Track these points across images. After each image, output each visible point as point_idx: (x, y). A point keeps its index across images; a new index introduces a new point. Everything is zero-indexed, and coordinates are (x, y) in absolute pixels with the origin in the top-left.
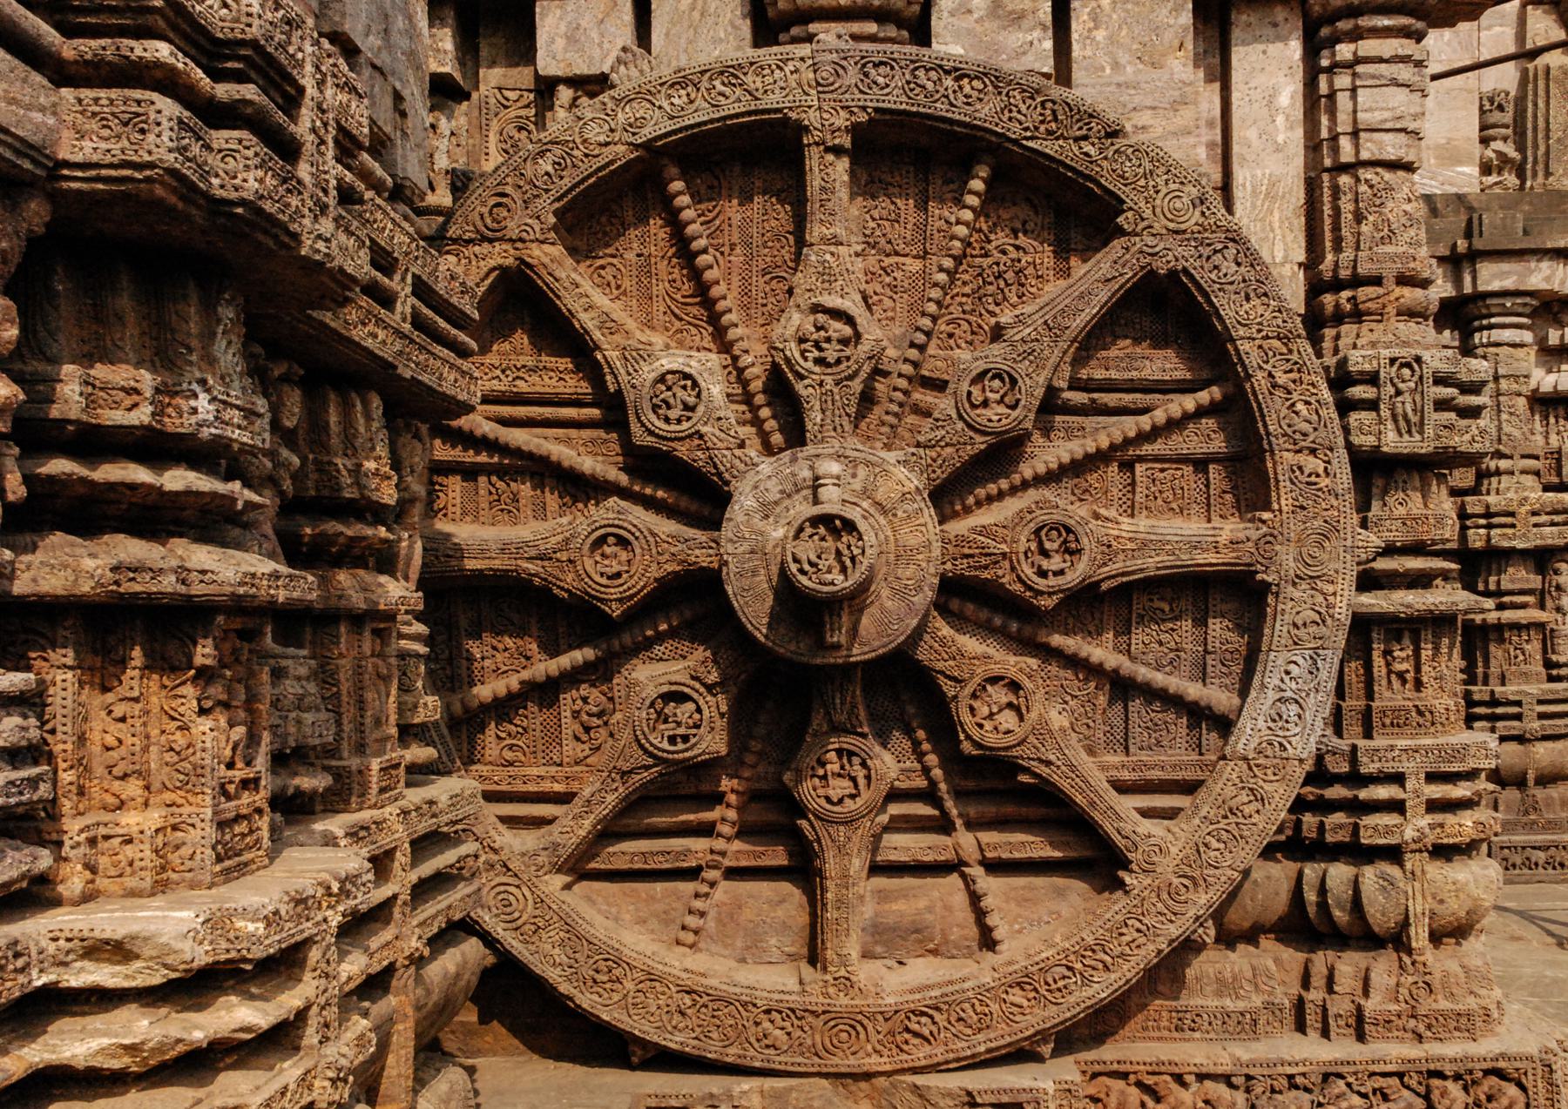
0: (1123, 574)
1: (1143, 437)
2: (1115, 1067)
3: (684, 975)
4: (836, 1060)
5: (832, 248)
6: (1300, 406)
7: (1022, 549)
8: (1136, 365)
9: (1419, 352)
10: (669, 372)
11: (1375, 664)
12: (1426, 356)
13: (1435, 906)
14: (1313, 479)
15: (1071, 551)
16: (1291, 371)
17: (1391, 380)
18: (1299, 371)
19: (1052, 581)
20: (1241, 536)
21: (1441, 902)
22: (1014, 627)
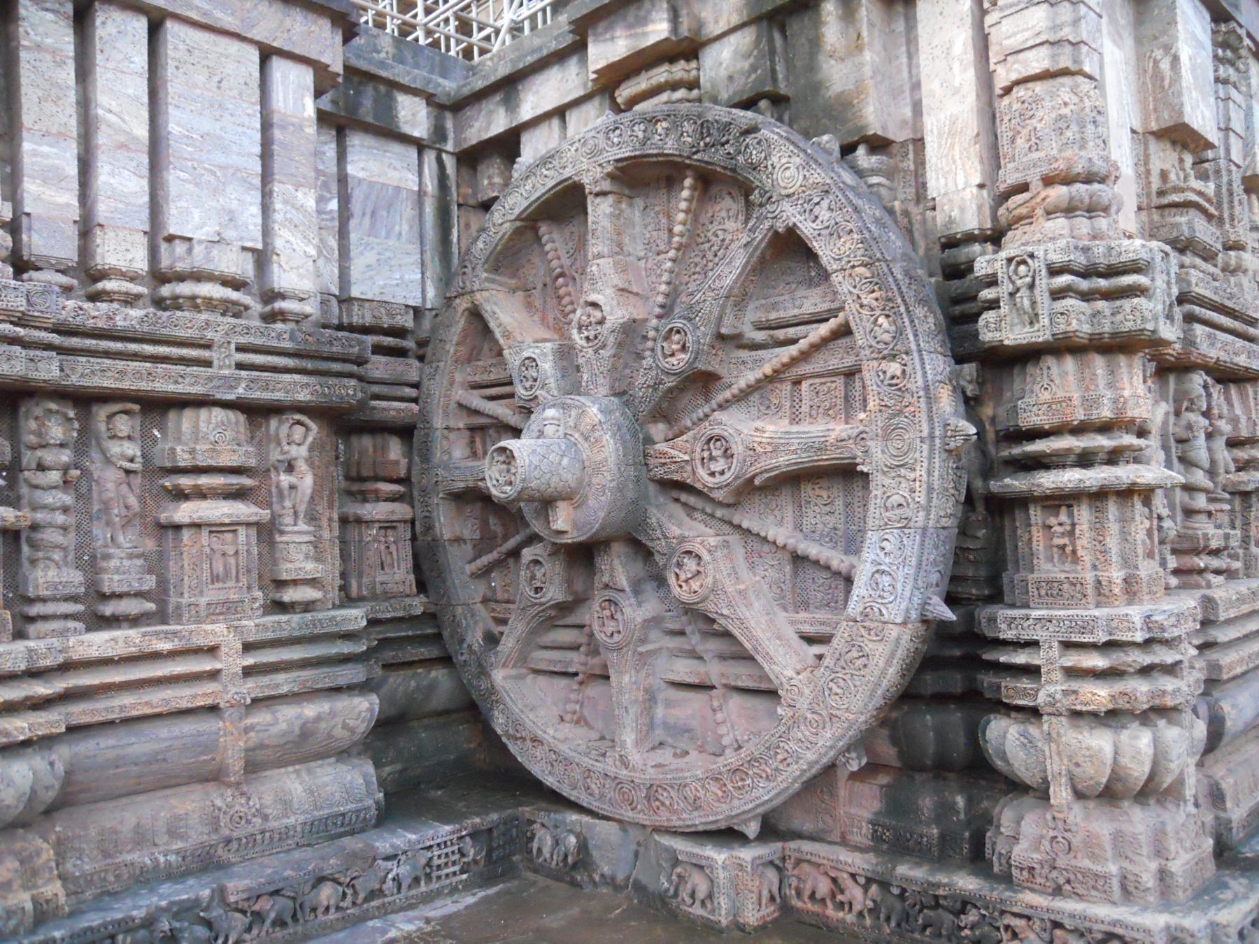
0: (766, 471)
1: (794, 361)
2: (809, 857)
3: (551, 740)
4: (623, 812)
5: (598, 261)
6: (881, 320)
7: (697, 456)
8: (797, 303)
9: (1030, 249)
10: (528, 358)
11: (1035, 539)
12: (1039, 252)
13: (1072, 768)
14: (894, 381)
15: (727, 454)
16: (873, 291)
17: (1010, 278)
18: (880, 289)
19: (718, 479)
20: (844, 435)
21: (1077, 765)
22: (719, 513)
